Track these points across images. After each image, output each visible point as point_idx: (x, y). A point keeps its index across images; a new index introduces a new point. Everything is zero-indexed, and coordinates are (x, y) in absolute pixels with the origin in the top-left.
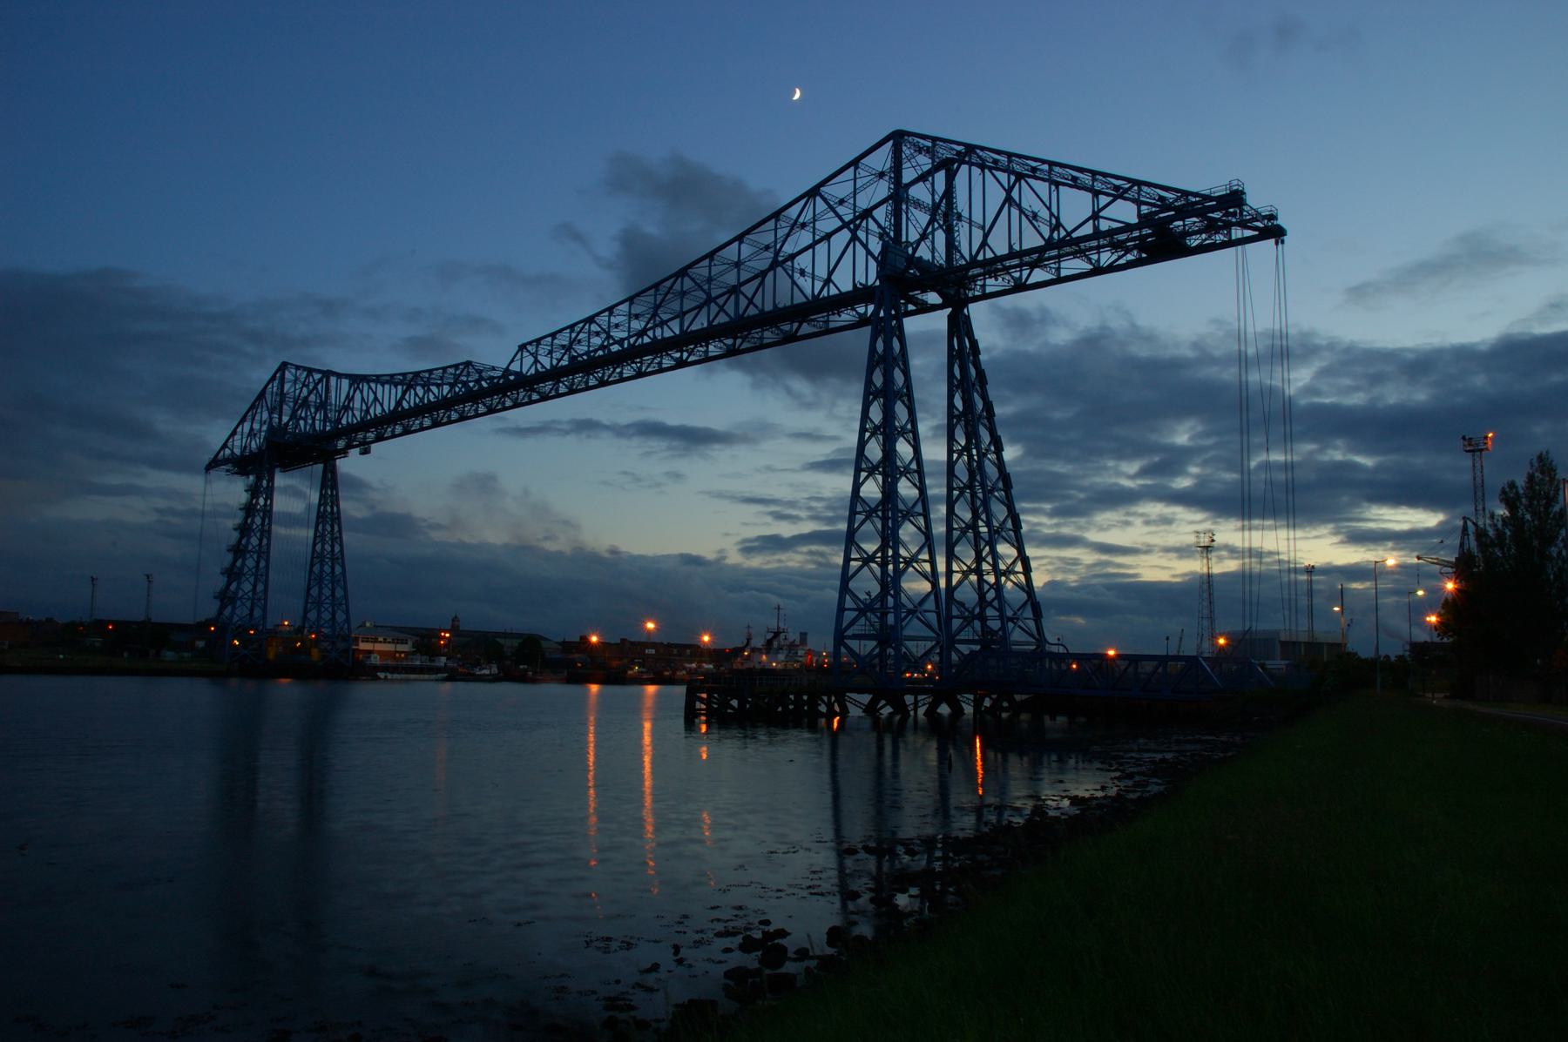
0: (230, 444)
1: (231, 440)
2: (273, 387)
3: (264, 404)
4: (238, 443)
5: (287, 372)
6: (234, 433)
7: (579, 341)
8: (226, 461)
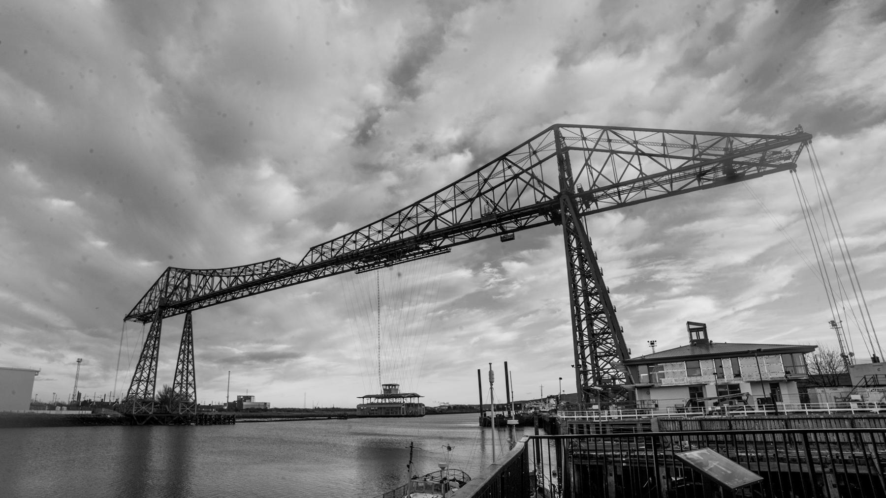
0: (138, 307)
1: (138, 305)
2: (162, 280)
3: (158, 288)
4: (142, 307)
6: (140, 302)
7: (274, 267)
8: (135, 316)
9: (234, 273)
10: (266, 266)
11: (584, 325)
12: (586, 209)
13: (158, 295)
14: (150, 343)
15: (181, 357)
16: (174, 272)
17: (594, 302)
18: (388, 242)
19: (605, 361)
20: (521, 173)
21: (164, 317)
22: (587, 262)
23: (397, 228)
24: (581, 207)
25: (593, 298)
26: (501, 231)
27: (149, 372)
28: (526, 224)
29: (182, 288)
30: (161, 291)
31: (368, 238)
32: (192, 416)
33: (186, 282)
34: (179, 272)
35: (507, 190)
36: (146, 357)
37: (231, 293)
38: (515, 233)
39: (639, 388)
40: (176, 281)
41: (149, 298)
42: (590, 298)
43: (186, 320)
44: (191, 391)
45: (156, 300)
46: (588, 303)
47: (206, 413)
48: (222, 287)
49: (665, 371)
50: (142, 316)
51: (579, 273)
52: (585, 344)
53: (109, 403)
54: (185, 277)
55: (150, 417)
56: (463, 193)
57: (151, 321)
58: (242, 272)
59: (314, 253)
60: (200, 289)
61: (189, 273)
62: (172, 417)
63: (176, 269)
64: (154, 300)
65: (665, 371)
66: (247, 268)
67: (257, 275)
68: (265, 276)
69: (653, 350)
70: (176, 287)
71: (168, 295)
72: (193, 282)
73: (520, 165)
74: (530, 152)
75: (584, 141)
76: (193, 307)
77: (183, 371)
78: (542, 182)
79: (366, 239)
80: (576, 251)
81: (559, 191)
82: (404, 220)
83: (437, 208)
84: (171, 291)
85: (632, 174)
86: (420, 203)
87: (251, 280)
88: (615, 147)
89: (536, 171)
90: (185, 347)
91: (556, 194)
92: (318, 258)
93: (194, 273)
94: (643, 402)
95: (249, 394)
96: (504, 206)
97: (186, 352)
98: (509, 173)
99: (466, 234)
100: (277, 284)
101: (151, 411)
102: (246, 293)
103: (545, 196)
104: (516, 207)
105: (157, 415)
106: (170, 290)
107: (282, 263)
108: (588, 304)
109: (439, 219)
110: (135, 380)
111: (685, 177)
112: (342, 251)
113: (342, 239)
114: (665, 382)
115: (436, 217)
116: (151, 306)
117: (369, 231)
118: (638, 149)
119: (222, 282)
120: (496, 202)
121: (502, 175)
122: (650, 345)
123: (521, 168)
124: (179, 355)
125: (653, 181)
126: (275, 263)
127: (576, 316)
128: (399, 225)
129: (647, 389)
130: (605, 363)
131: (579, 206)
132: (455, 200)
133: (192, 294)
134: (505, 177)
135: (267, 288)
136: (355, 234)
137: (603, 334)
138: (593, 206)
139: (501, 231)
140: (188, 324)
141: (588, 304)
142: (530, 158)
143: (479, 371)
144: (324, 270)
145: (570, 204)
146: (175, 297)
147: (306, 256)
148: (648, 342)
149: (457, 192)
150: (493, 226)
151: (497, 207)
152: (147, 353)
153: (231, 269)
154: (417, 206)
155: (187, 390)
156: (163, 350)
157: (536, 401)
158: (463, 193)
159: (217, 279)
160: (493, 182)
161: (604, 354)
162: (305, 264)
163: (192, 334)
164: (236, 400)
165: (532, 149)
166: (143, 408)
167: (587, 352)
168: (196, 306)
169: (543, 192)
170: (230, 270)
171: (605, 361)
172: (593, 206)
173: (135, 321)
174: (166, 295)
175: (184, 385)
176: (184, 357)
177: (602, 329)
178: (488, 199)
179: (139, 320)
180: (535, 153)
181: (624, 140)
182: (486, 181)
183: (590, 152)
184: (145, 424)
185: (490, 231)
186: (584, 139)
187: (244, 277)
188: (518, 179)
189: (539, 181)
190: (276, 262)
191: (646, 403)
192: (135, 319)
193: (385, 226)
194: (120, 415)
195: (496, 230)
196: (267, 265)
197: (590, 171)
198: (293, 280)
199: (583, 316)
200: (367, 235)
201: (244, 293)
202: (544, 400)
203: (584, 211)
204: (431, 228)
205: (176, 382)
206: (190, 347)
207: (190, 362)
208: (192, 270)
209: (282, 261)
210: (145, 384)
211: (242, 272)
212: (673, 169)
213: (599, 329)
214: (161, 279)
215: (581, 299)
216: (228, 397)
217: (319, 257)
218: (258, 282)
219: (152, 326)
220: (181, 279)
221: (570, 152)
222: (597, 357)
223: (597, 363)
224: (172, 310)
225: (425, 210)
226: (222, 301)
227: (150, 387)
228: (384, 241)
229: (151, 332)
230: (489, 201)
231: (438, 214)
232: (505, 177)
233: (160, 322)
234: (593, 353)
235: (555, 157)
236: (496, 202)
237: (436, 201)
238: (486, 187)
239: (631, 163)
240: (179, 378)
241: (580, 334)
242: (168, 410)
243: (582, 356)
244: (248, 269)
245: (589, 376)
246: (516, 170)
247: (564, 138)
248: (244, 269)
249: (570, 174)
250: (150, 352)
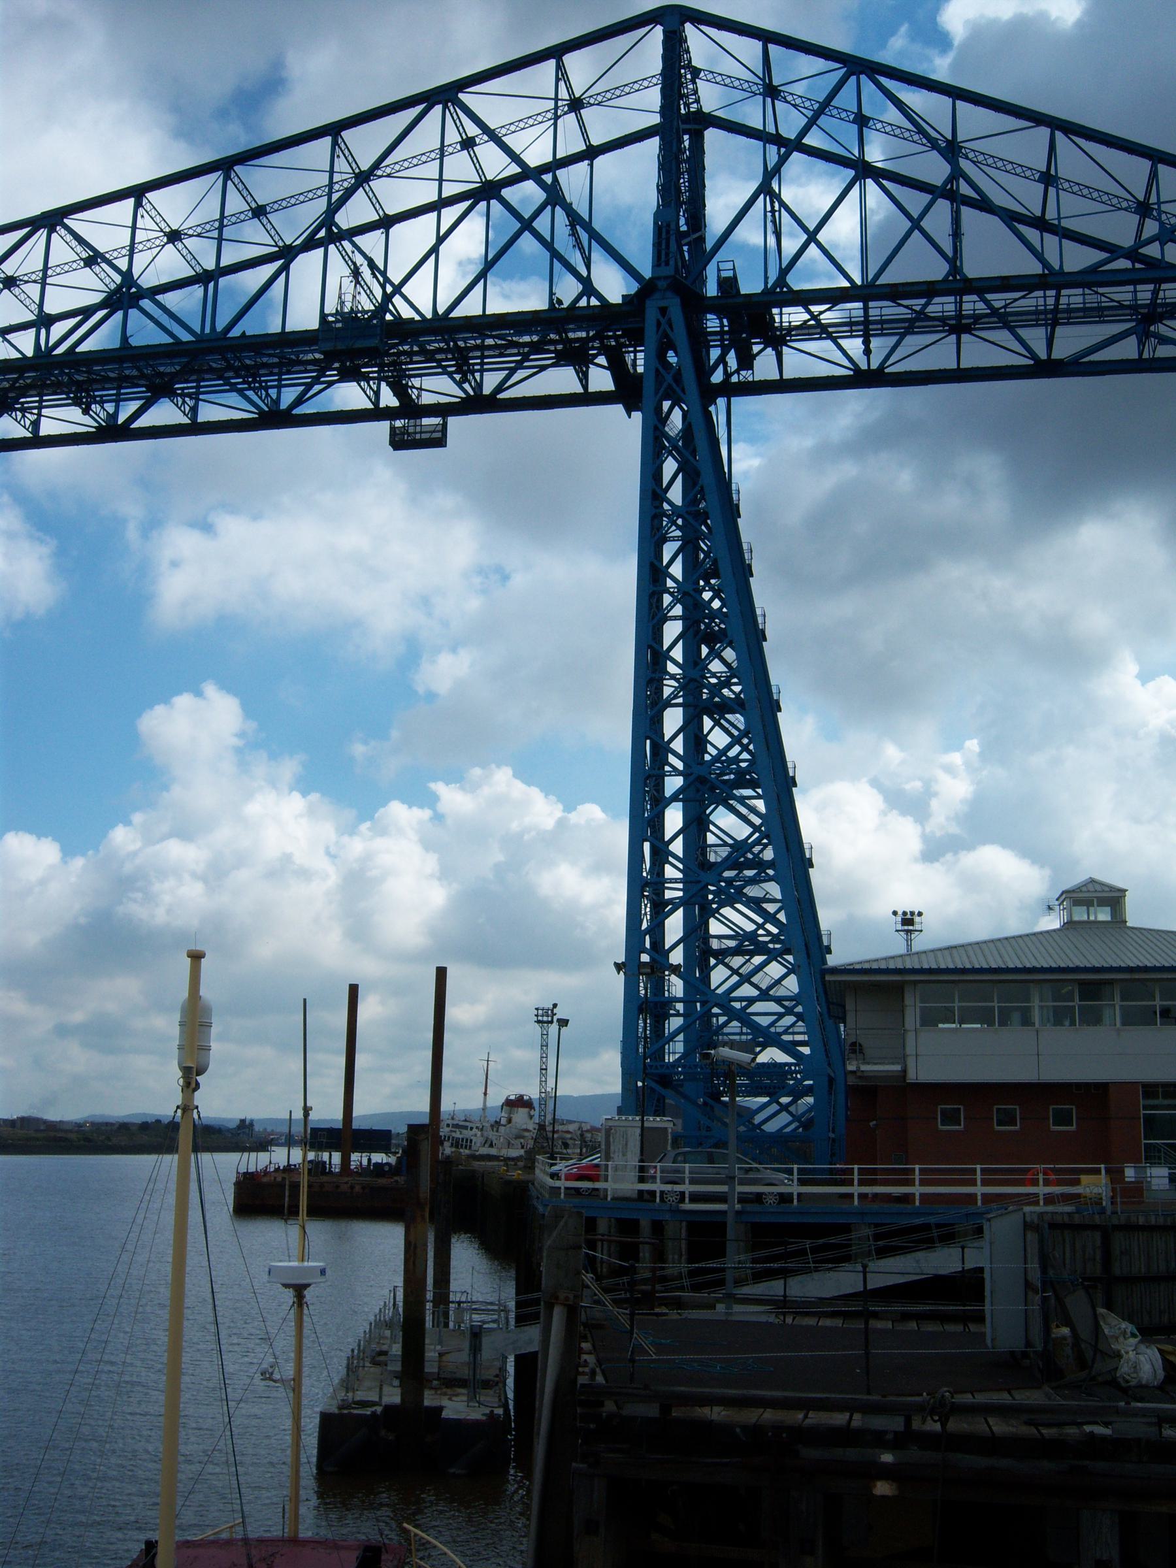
11: (674, 818)
12: (737, 372)
17: (719, 739)
19: (735, 972)
24: (722, 360)
25: (717, 723)
28: (500, 388)
35: (441, 239)
38: (451, 420)
42: (707, 723)
51: (678, 610)
52: (669, 895)
56: (259, 212)
69: (909, 942)
75: (769, 100)
78: (588, 226)
81: (647, 273)
86: (65, 221)
89: (573, 180)
99: (250, 393)
103: (588, 288)
108: (696, 741)
111: (1096, 314)
118: (957, 174)
120: (396, 277)
122: (900, 927)
123: (515, 158)
130: (735, 978)
131: (715, 354)
132: (220, 240)
134: (441, 180)
138: (765, 366)
141: (696, 741)
142: (555, 125)
145: (680, 334)
148: (895, 913)
149: (236, 203)
150: (367, 379)
158: (259, 212)
161: (732, 944)
165: (569, 88)
167: (675, 925)
169: (584, 273)
171: (735, 972)
172: (765, 366)
178: (359, 259)
180: (576, 105)
182: (363, 178)
186: (771, 92)
188: (493, 202)
189: (574, 219)
195: (377, 394)
197: (774, 222)
199: (673, 784)
203: (727, 375)
213: (725, 844)
215: (673, 720)
221: (712, 136)
223: (706, 979)
234: (696, 933)
235: (653, 145)
236: (396, 277)
239: (909, 224)
241: (654, 852)
245: (675, 1023)
246: (495, 164)
247: (696, 72)
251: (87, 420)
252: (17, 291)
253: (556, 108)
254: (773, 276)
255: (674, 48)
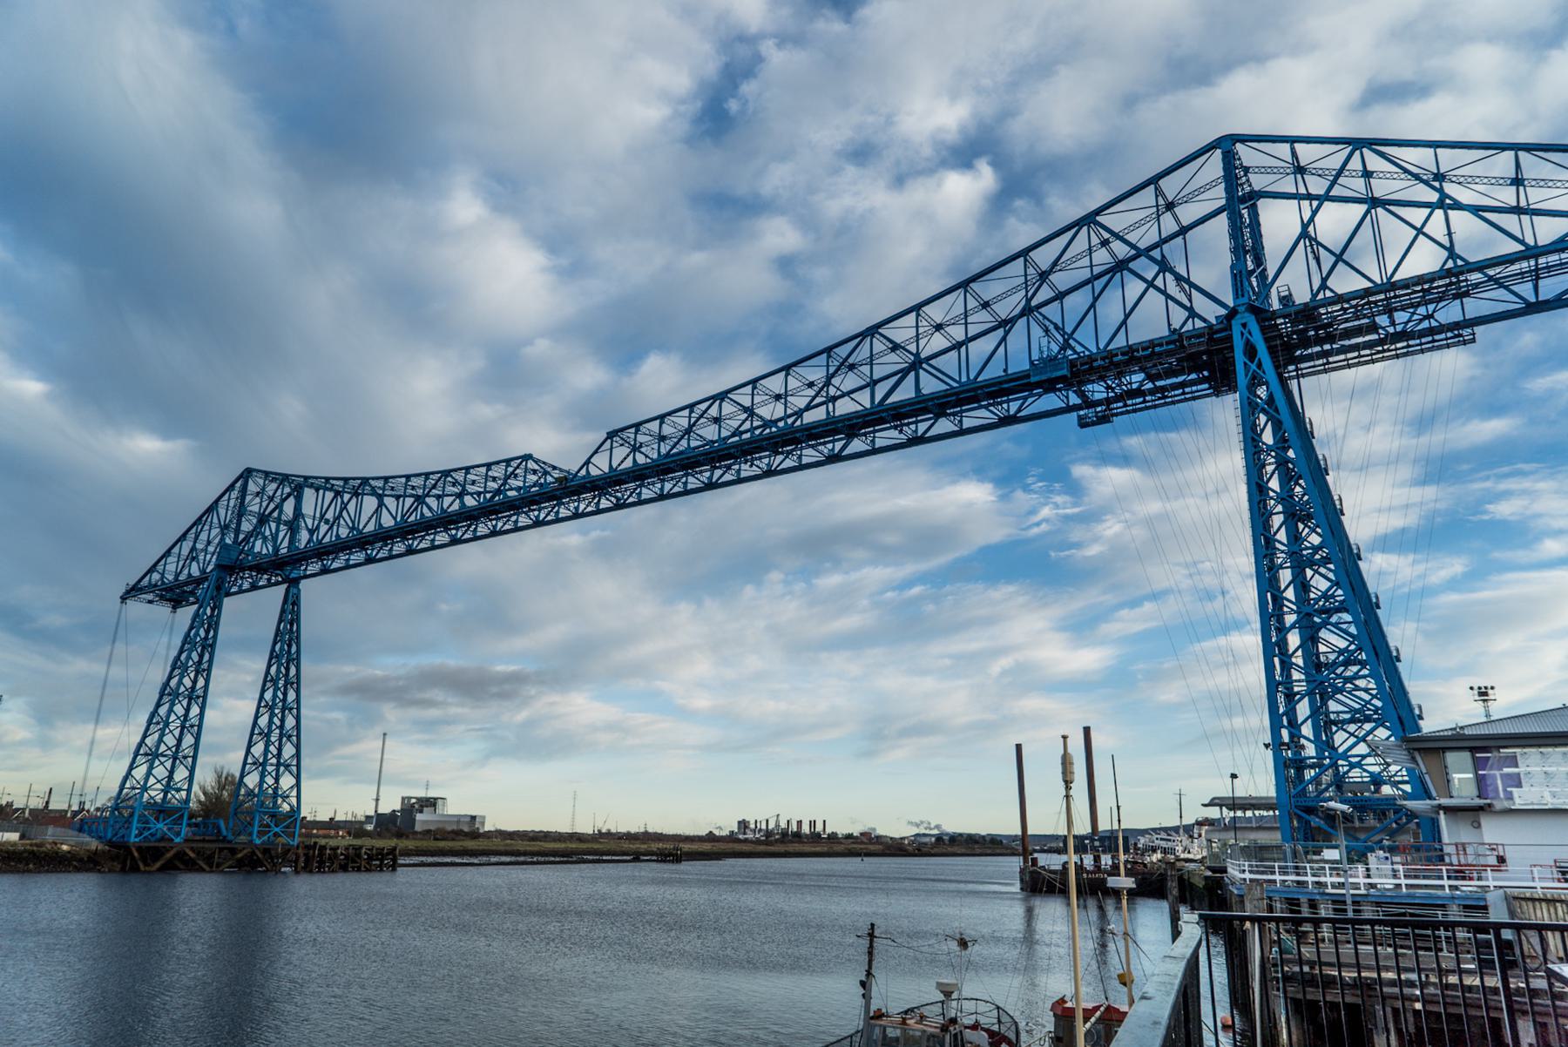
0: (160, 568)
1: (163, 562)
2: (229, 499)
3: (215, 520)
4: (171, 568)
5: (250, 481)
6: (168, 553)
7: (516, 476)
8: (152, 587)
9: (413, 488)
10: (496, 475)
11: (1294, 640)
13: (215, 538)
14: (189, 657)
15: (268, 695)
16: (261, 482)
17: (1320, 584)
18: (798, 423)
19: (1352, 734)
20: (1134, 258)
21: (228, 594)
22: (1301, 481)
23: (822, 389)
25: (1316, 572)
26: (1078, 401)
27: (181, 733)
29: (278, 521)
30: (224, 528)
31: (750, 411)
32: (287, 849)
33: (289, 507)
34: (274, 480)
35: (1096, 299)
36: (175, 695)
37: (404, 538)
39: (1450, 810)
40: (264, 504)
41: (191, 544)
42: (1309, 573)
43: (285, 601)
44: (287, 781)
45: (211, 549)
46: (1302, 583)
47: (323, 842)
48: (382, 522)
49: (1521, 769)
50: (170, 589)
51: (1280, 508)
52: (1296, 689)
53: (66, 812)
54: (289, 495)
55: (175, 850)
56: (986, 305)
57: (193, 603)
58: (434, 487)
59: (615, 444)
60: (327, 527)
61: (298, 485)
62: (233, 851)
63: (267, 474)
64: (205, 550)
65: (1521, 769)
66: (447, 476)
67: (472, 494)
68: (493, 497)
70: (263, 519)
71: (241, 537)
72: (308, 508)
73: (1132, 238)
74: (1157, 206)
75: (1299, 176)
76: (306, 569)
77: (270, 731)
78: (1188, 281)
79: (746, 415)
80: (1273, 454)
82: (838, 369)
83: (922, 343)
84: (251, 528)
85: (1425, 260)
86: (880, 330)
87: (456, 506)
88: (1381, 189)
89: (1173, 251)
90: (278, 671)
91: (1223, 312)
92: (625, 458)
93: (311, 486)
94: (1461, 847)
95: (432, 794)
96: (1087, 342)
97: (281, 683)
98: (1102, 257)
99: (991, 408)
100: (520, 519)
101: (178, 834)
102: (442, 538)
103: (1192, 314)
104: (1120, 342)
105: (194, 845)
106: (246, 526)
107: (536, 467)
108: (1303, 587)
109: (924, 370)
110: (142, 752)
112: (684, 443)
113: (686, 412)
114: (1523, 797)
115: (917, 364)
116: (194, 564)
117: (753, 395)
118: (1443, 195)
119: (384, 509)
120: (1068, 330)
121: (1086, 261)
124: (263, 691)
125: (1486, 275)
126: (518, 467)
127: (1271, 618)
128: (828, 383)
129: (1472, 813)
130: (1352, 740)
132: (966, 324)
133: (304, 536)
134: (1091, 266)
135: (495, 527)
136: (718, 402)
137: (1347, 664)
139: (1078, 401)
140: (291, 611)
141: (1303, 587)
142: (1158, 220)
143: (1019, 748)
144: (638, 486)
146: (259, 543)
147: (596, 452)
149: (972, 303)
150: (1060, 390)
151: (1071, 341)
152: (180, 683)
153: (408, 477)
154: (873, 336)
155: (277, 780)
156: (220, 677)
157: (1166, 830)
158: (986, 305)
159: (370, 503)
160: (1061, 280)
161: (1347, 716)
162: (594, 472)
163: (298, 638)
164: (398, 807)
165: (1164, 197)
166: (160, 826)
167: (1303, 709)
168: (314, 567)
169: (1189, 305)
170: (403, 480)
171: (1352, 734)
173: (150, 602)
174: (237, 536)
175: (270, 769)
176: (275, 696)
177: (1341, 652)
178: (1047, 323)
179: (162, 598)
180: (1170, 206)
181: (1406, 171)
182: (1044, 276)
183: (1315, 203)
184: (161, 869)
185: (1051, 401)
186: (1300, 170)
187: (438, 497)
188: (1125, 272)
190: (521, 463)
191: (1469, 850)
192: (150, 597)
193: (793, 383)
194: (94, 844)
195: (1067, 397)
196: (498, 472)
197: (1313, 252)
198: (561, 510)
199: (1290, 619)
200: (747, 403)
201: (437, 538)
202: (1188, 830)
204: (905, 392)
205: (250, 761)
206: (293, 671)
207: (291, 709)
208: (306, 478)
209: (537, 461)
210: (168, 764)
211: (434, 487)
212: (1540, 243)
213: (1334, 651)
214: (226, 497)
215: (1286, 576)
216: (377, 800)
217: (628, 455)
218: (475, 513)
219: (196, 615)
220: (277, 500)
222: (1330, 723)
224: (251, 577)
225: (890, 346)
226: (379, 556)
227: (181, 774)
228: (790, 421)
229: (193, 631)
230: (1051, 327)
231: (923, 356)
232: (1091, 266)
233: (217, 607)
234: (1317, 712)
235: (1224, 216)
236: (1068, 330)
237: (920, 324)
238: (1045, 293)
239: (1415, 232)
240: (258, 750)
241: (1282, 662)
242: (224, 832)
243: (1289, 722)
244: (449, 479)
246: (1121, 250)
247: (1247, 170)
248: (440, 478)
249: (1259, 260)
250: (187, 682)
251: (902, 436)
252: (856, 371)
253: (1158, 210)
254: (1316, 284)
255: (1230, 159)
